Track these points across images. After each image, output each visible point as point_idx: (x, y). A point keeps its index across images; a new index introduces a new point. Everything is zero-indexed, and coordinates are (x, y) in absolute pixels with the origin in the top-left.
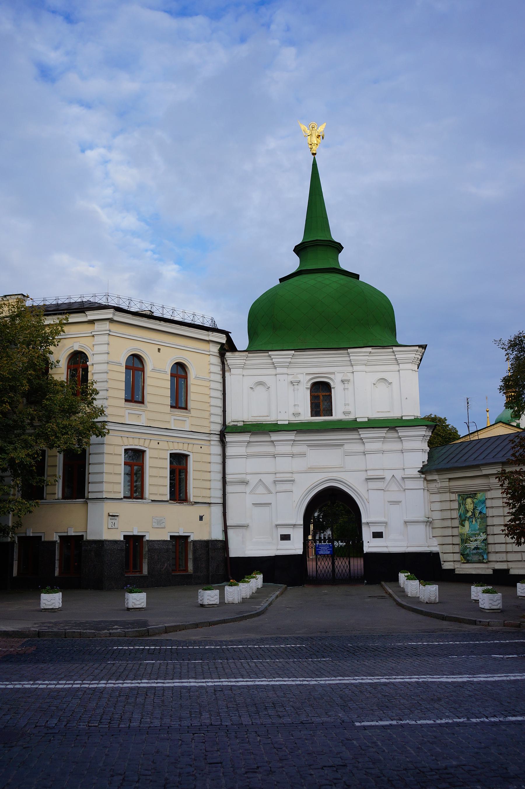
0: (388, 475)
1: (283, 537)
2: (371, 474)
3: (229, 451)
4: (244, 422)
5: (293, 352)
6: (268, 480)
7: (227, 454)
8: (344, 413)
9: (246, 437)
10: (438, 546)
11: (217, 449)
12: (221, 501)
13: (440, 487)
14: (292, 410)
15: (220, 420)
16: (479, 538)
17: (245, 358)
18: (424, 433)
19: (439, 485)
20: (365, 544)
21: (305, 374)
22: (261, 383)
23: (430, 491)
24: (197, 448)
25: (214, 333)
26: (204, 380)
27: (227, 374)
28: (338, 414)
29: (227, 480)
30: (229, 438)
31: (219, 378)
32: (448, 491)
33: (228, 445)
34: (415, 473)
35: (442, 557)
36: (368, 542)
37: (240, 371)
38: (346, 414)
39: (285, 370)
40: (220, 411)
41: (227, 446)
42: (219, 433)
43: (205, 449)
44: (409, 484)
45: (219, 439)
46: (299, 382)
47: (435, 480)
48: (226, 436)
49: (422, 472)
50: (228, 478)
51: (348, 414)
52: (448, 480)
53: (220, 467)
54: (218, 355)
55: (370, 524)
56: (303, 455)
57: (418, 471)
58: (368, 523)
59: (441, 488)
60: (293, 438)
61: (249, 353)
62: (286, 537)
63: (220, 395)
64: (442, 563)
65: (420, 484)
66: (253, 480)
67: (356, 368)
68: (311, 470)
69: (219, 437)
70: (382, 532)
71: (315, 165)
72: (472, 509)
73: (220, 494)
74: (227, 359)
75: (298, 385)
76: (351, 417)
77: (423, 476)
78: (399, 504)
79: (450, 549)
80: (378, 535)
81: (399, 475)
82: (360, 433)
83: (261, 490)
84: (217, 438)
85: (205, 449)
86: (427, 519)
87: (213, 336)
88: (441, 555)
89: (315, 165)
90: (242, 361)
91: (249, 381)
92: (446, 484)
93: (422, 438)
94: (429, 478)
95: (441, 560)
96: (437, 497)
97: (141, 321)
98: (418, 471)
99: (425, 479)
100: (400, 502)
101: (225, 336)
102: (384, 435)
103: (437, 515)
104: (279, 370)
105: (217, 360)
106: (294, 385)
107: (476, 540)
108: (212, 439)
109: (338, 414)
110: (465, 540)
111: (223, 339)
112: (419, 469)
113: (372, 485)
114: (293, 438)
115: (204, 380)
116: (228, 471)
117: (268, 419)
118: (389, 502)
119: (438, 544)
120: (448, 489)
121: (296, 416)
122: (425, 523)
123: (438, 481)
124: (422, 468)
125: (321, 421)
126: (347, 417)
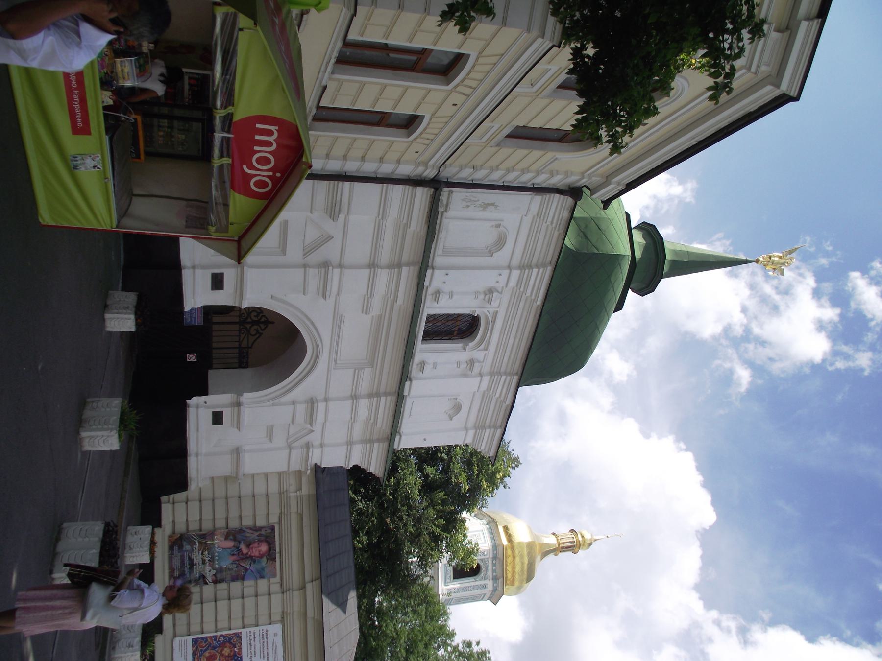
0: (317, 427)
2: (321, 406)
3: (397, 191)
6: (331, 251)
7: (391, 186)
11: (405, 170)
13: (290, 497)
14: (446, 288)
16: (208, 568)
19: (292, 495)
21: (498, 309)
22: (500, 242)
25: (618, 191)
28: (424, 351)
29: (341, 183)
30: (422, 195)
33: (408, 188)
34: (316, 457)
35: (180, 496)
36: (205, 403)
38: (420, 366)
39: (513, 283)
41: (407, 186)
44: (297, 455)
46: (489, 301)
47: (300, 489)
48: (426, 189)
49: (317, 468)
56: (366, 309)
57: (316, 464)
58: (238, 405)
59: (289, 498)
62: (217, 282)
64: (172, 496)
65: (296, 466)
66: (333, 228)
67: (486, 379)
68: (338, 320)
72: (253, 555)
75: (484, 299)
76: (414, 370)
77: (309, 472)
78: (267, 437)
79: (194, 516)
80: (218, 418)
81: (315, 438)
83: (312, 235)
87: (614, 188)
90: (550, 219)
92: (294, 509)
96: (274, 488)
97: (726, 119)
98: (316, 464)
100: (271, 440)
103: (246, 490)
104: (516, 273)
106: (486, 295)
107: (204, 562)
109: (424, 351)
110: (205, 538)
112: (319, 464)
113: (301, 409)
116: (358, 185)
117: (439, 251)
118: (272, 427)
120: (286, 512)
121: (434, 296)
124: (320, 467)
125: (417, 330)
126: (415, 366)
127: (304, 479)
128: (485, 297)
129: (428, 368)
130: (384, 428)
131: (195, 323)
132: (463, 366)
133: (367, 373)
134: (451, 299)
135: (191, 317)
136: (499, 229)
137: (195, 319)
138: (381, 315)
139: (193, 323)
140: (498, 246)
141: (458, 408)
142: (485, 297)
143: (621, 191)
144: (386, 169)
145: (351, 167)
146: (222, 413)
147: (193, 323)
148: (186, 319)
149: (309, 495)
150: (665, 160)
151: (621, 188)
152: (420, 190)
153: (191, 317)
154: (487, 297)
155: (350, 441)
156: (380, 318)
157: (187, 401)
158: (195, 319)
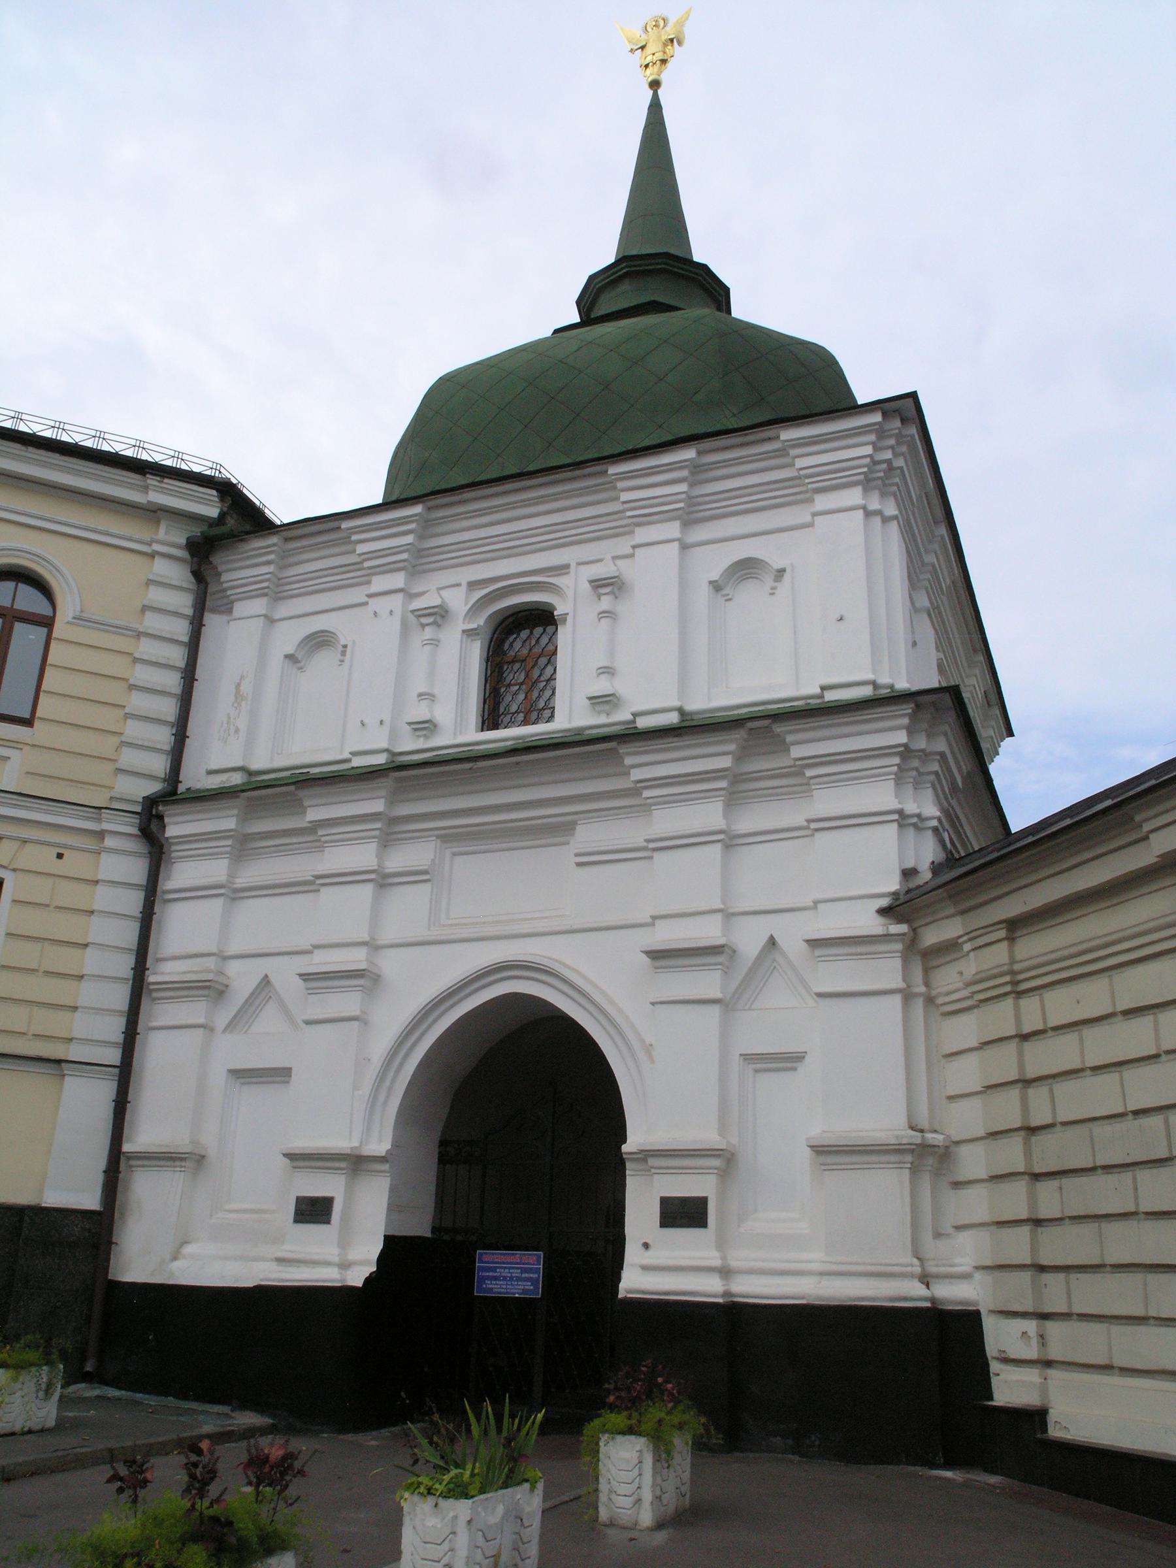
1: (304, 1207)
2: (668, 935)
4: (250, 773)
5: (418, 509)
8: (600, 701)
9: (226, 820)
10: (978, 1276)
11: (135, 869)
12: (113, 1056)
13: (977, 973)
15: (159, 765)
17: (272, 557)
18: (901, 737)
20: (633, 1254)
23: (940, 1001)
24: (43, 858)
25: (166, 480)
26: (118, 629)
27: (210, 619)
30: (177, 826)
31: (181, 629)
32: (1008, 988)
33: (176, 851)
34: (867, 921)
37: (258, 606)
38: (598, 708)
40: (164, 737)
41: (174, 855)
42: (138, 809)
43: (74, 864)
45: (135, 831)
48: (166, 820)
50: (160, 973)
51: (606, 707)
52: (1002, 934)
53: (128, 934)
54: (183, 554)
55: (652, 1161)
57: (883, 912)
60: (378, 806)
61: (287, 540)
63: (173, 682)
69: (138, 821)
70: (703, 1202)
71: (655, 108)
73: (114, 1028)
74: (220, 569)
75: (435, 623)
76: (623, 715)
78: (795, 1069)
82: (628, 761)
84: (130, 826)
85: (74, 864)
86: (916, 1138)
87: (163, 491)
88: (989, 1324)
89: (655, 108)
91: (288, 637)
92: (998, 955)
93: (897, 760)
94: (931, 936)
95: (991, 1350)
98: (883, 912)
99: (911, 947)
100: (799, 1057)
101: (214, 492)
102: (726, 762)
105: (178, 573)
108: (105, 826)
111: (209, 507)
112: (885, 902)
114: (378, 806)
115: (118, 629)
119: (977, 1268)
120: (1007, 978)
122: (909, 1158)
123: (967, 947)
126: (603, 719)
127: (931, 936)
128: (428, 625)
129: (602, 686)
130: (732, 747)
131: (537, 1271)
132: (606, 603)
133: (589, 835)
134: (434, 696)
135: (519, 1279)
136: (300, 656)
137: (524, 1270)
138: (438, 837)
139: (536, 1276)
140: (329, 639)
141: (746, 569)
142: (428, 625)
143: (164, 477)
144: (133, 902)
145: (124, 965)
146: (665, 1201)
147: (536, 1276)
148: (524, 1291)
149: (962, 913)
150: (23, 448)
151: (152, 481)
152: (172, 831)
153: (519, 1279)
154: (424, 620)
155: (808, 828)
156: (447, 838)
157: (620, 1296)
158: (524, 1270)
